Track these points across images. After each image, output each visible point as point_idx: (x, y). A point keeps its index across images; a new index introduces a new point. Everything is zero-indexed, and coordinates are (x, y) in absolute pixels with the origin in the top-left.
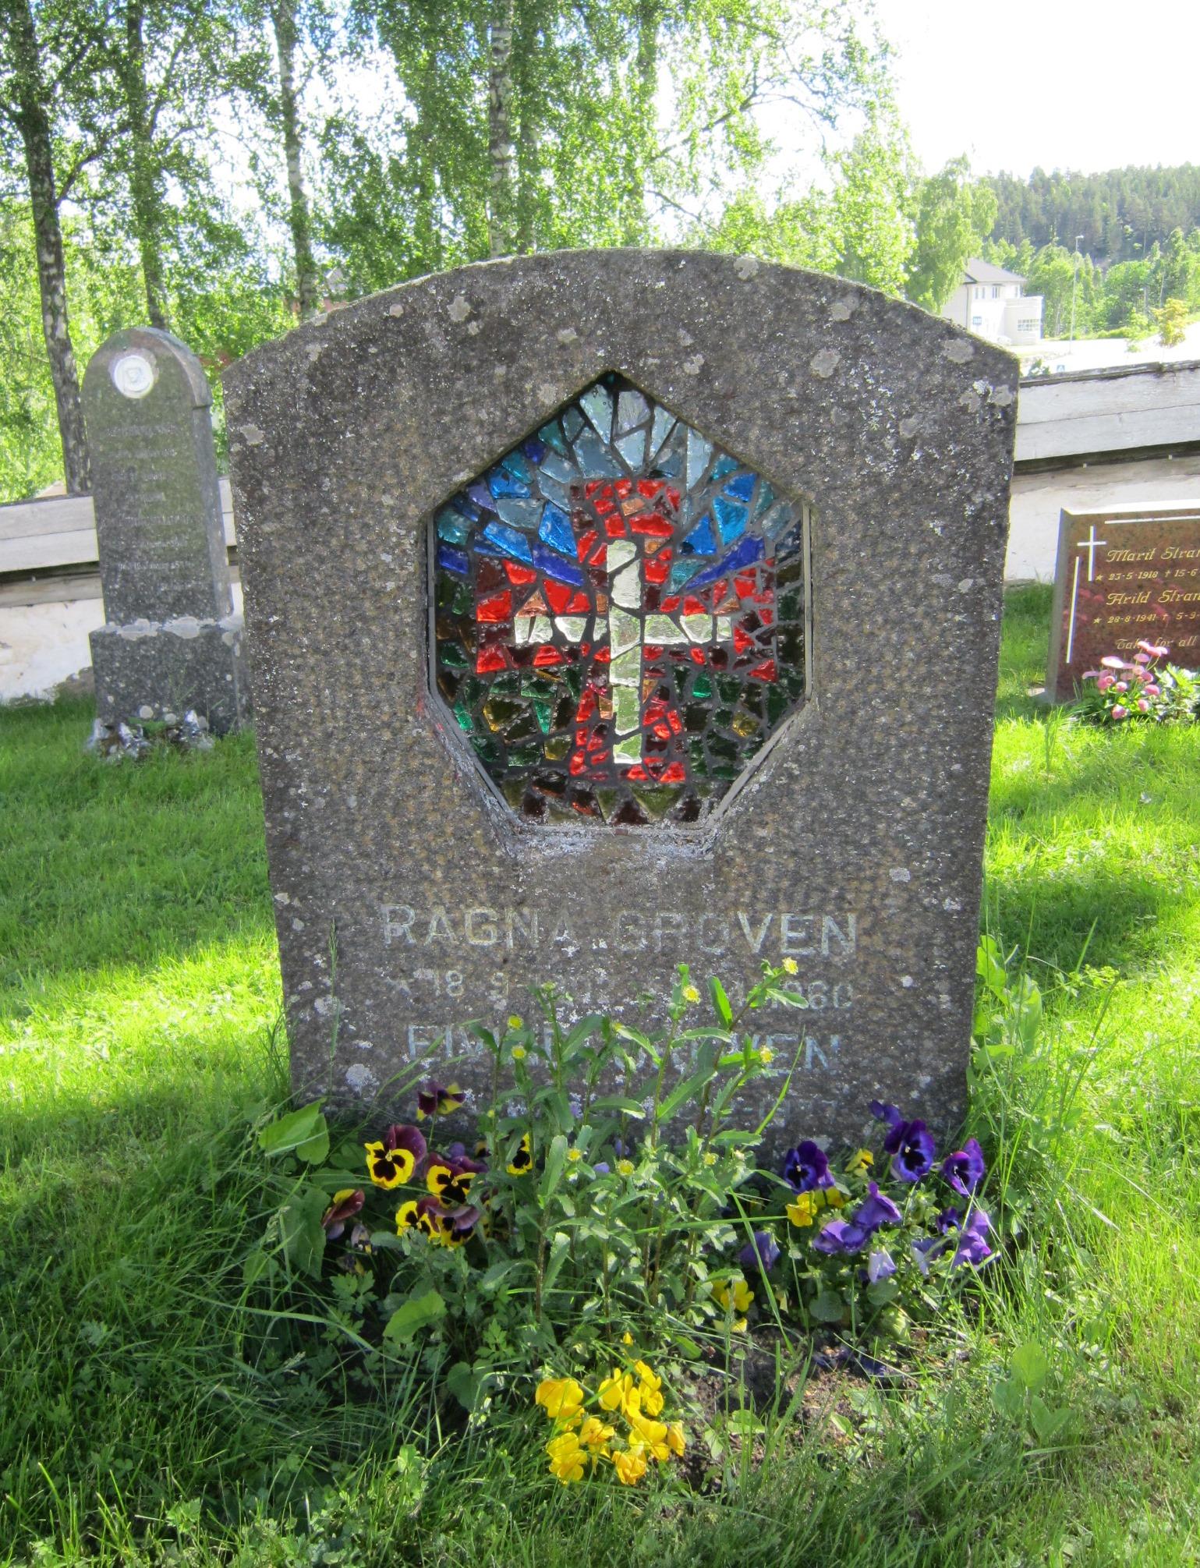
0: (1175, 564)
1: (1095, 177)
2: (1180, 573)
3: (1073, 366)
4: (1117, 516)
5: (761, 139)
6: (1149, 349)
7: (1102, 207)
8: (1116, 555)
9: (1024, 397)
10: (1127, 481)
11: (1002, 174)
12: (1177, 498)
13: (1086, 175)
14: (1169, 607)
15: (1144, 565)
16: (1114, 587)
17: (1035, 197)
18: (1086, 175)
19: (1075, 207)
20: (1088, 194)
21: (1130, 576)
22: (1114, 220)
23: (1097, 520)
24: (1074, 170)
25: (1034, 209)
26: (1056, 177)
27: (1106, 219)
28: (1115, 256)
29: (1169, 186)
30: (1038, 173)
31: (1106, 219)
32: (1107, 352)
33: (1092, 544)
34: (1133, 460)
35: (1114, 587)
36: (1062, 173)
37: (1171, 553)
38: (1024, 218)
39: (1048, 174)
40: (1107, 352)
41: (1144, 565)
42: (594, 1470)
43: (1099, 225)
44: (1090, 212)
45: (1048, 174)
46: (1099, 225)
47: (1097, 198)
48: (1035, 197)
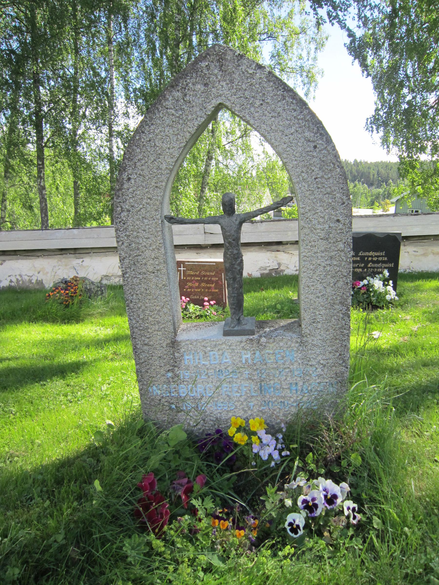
0: (204, 276)
1: (371, 163)
2: (206, 279)
3: (363, 214)
4: (188, 262)
5: (251, 148)
6: (379, 212)
7: (373, 172)
8: (189, 272)
9: (354, 221)
10: (251, 251)
11: (346, 160)
12: (211, 258)
13: (369, 162)
14: (203, 288)
15: (195, 276)
16: (189, 281)
17: (354, 168)
18: (369, 162)
19: (365, 171)
20: (369, 168)
21: (193, 278)
22: (376, 176)
23: (183, 262)
24: (366, 161)
25: (354, 171)
26: (361, 162)
27: (374, 175)
28: (376, 186)
29: (392, 168)
30: (355, 161)
31: (374, 175)
32: (368, 212)
33: (182, 269)
34: (253, 246)
35: (189, 281)
36: (362, 161)
37: (203, 273)
38: (351, 173)
39: (358, 161)
40: (368, 212)
41: (195, 276)
42: (128, 567)
43: (372, 177)
44: (369, 173)
45: (358, 161)
46: (372, 177)
47: (372, 169)
48: (354, 167)
